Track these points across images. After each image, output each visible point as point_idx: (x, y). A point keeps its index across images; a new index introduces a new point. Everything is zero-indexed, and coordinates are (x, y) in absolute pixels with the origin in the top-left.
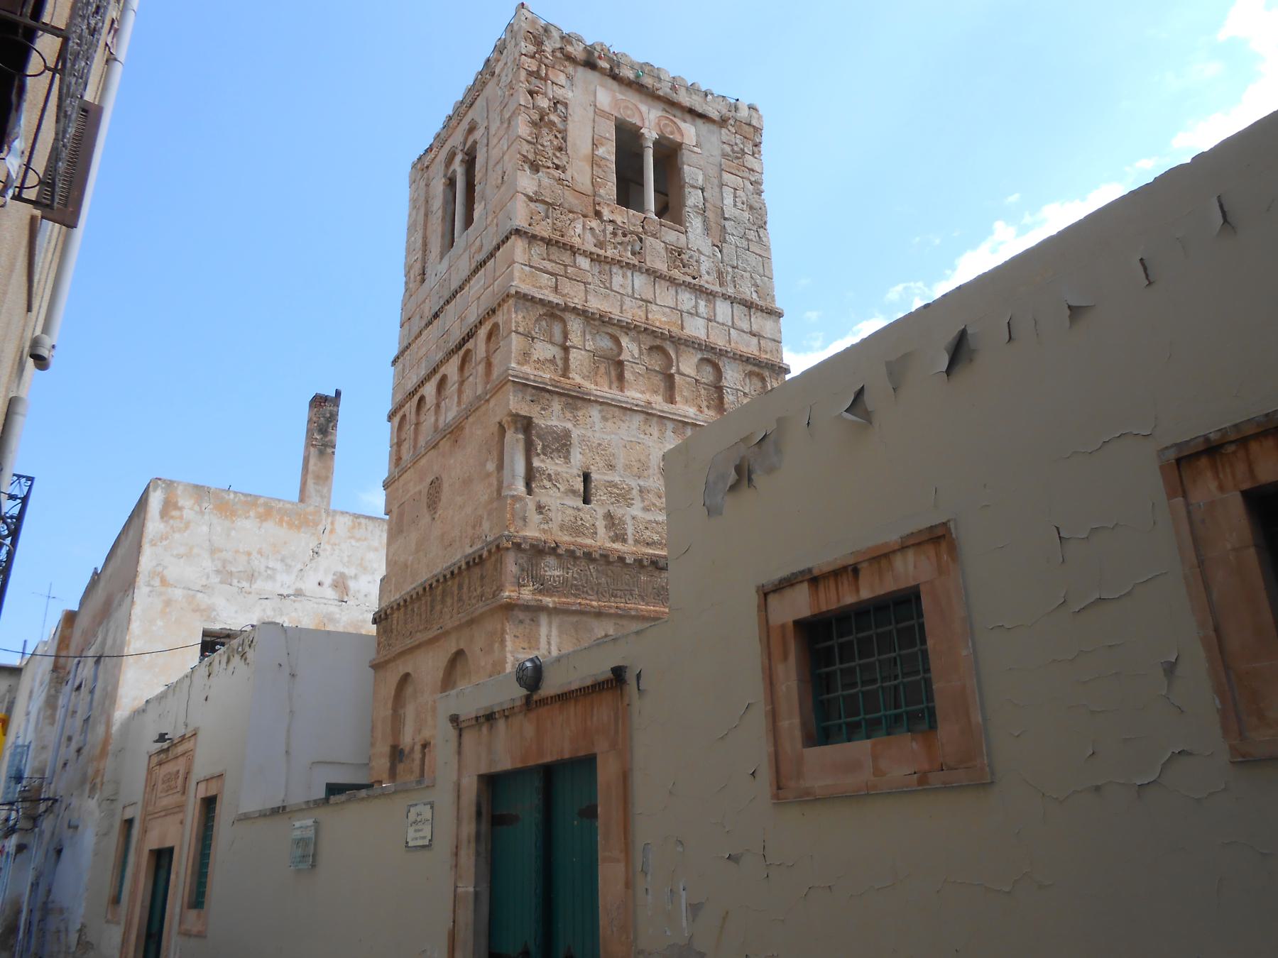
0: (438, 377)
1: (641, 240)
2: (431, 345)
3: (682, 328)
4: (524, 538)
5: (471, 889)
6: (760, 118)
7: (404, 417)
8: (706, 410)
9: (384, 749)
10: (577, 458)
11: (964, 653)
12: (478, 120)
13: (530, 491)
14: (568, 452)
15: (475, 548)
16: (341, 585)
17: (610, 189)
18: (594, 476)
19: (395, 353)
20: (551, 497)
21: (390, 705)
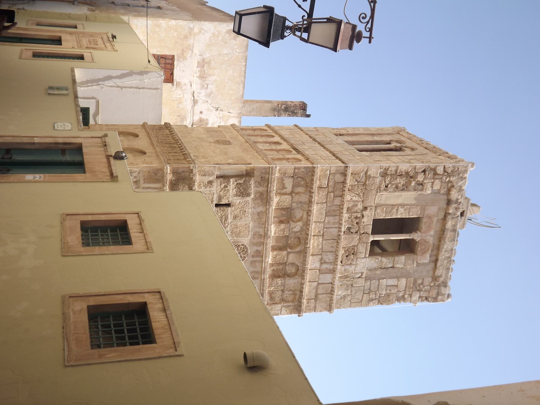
1: (356, 232)
3: (312, 255)
4: (195, 175)
6: (443, 301)
7: (266, 130)
8: (272, 269)
10: (237, 201)
13: (218, 177)
14: (240, 196)
18: (229, 209)
19: (301, 126)
20: (216, 188)
21: (124, 130)
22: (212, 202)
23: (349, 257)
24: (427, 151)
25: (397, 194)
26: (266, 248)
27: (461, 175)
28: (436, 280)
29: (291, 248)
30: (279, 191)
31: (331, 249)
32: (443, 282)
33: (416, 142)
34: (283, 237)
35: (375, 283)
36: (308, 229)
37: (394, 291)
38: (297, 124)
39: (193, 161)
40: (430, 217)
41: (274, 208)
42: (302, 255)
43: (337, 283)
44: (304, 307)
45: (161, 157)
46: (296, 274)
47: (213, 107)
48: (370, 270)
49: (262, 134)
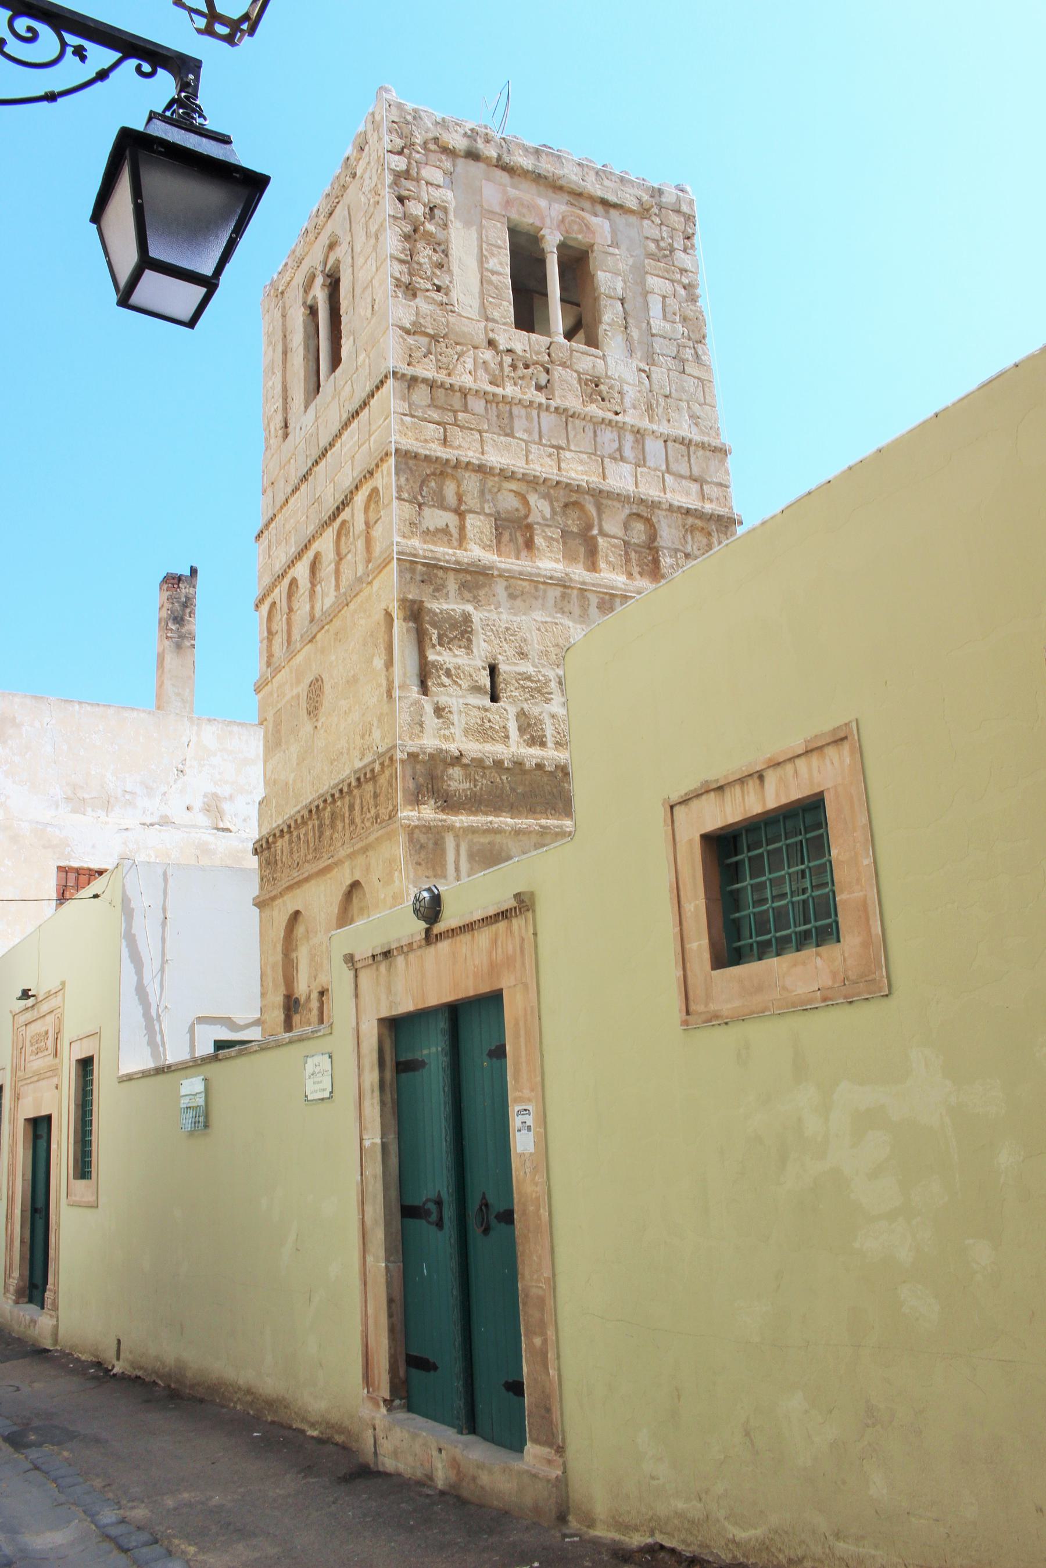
0: (310, 555)
1: (547, 371)
2: (301, 516)
5: (378, 1141)
6: (691, 203)
8: (638, 577)
9: (279, 999)
10: (482, 648)
11: (866, 862)
12: (339, 232)
13: (424, 689)
14: (469, 640)
15: (366, 761)
16: (213, 807)
17: (506, 309)
18: (502, 667)
19: (259, 526)
20: (451, 696)
22: (486, 710)
23: (605, 394)
24: (340, 212)
25: (455, 268)
26: (593, 585)
27: (409, 118)
28: (647, 210)
29: (589, 527)
30: (455, 543)
31: (591, 434)
32: (652, 197)
33: (312, 244)
34: (565, 543)
35: (658, 345)
36: (545, 480)
37: (673, 304)
38: (256, 534)
39: (380, 755)
40: (508, 203)
41: (495, 557)
42: (604, 501)
43: (664, 428)
44: (721, 511)
45: (372, 838)
46: (648, 521)
47: (175, 781)
48: (631, 352)
49: (285, 609)
